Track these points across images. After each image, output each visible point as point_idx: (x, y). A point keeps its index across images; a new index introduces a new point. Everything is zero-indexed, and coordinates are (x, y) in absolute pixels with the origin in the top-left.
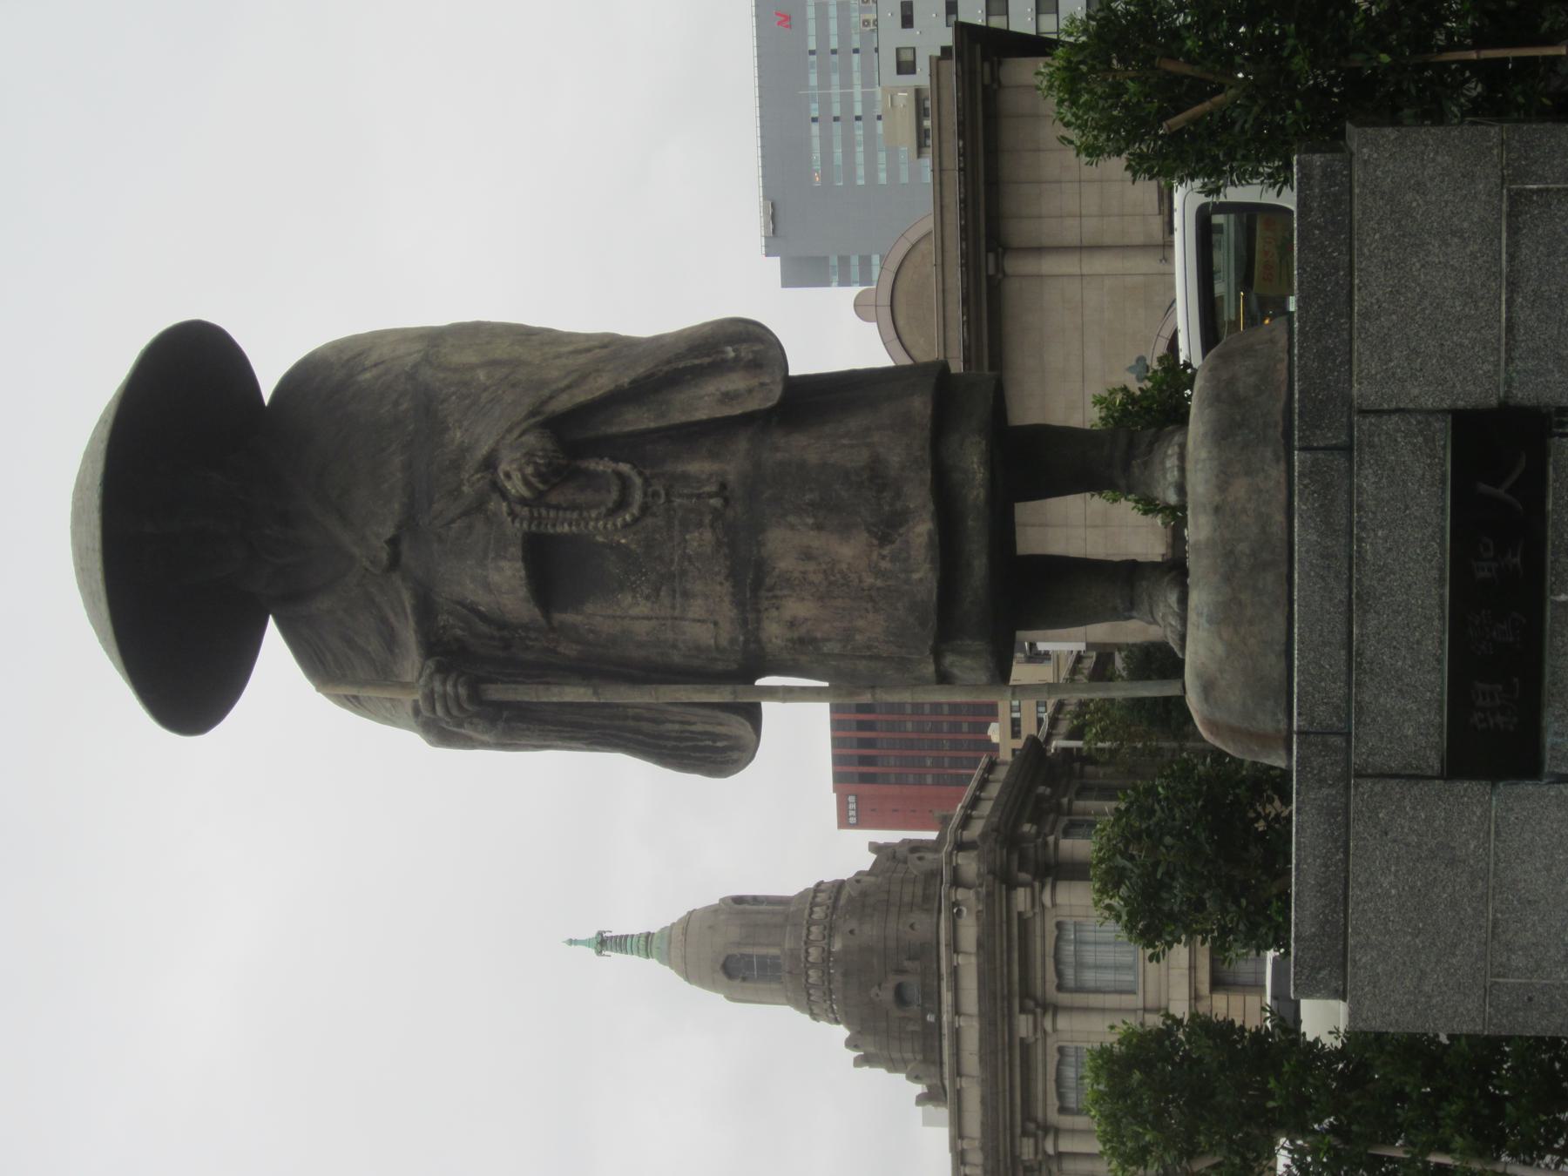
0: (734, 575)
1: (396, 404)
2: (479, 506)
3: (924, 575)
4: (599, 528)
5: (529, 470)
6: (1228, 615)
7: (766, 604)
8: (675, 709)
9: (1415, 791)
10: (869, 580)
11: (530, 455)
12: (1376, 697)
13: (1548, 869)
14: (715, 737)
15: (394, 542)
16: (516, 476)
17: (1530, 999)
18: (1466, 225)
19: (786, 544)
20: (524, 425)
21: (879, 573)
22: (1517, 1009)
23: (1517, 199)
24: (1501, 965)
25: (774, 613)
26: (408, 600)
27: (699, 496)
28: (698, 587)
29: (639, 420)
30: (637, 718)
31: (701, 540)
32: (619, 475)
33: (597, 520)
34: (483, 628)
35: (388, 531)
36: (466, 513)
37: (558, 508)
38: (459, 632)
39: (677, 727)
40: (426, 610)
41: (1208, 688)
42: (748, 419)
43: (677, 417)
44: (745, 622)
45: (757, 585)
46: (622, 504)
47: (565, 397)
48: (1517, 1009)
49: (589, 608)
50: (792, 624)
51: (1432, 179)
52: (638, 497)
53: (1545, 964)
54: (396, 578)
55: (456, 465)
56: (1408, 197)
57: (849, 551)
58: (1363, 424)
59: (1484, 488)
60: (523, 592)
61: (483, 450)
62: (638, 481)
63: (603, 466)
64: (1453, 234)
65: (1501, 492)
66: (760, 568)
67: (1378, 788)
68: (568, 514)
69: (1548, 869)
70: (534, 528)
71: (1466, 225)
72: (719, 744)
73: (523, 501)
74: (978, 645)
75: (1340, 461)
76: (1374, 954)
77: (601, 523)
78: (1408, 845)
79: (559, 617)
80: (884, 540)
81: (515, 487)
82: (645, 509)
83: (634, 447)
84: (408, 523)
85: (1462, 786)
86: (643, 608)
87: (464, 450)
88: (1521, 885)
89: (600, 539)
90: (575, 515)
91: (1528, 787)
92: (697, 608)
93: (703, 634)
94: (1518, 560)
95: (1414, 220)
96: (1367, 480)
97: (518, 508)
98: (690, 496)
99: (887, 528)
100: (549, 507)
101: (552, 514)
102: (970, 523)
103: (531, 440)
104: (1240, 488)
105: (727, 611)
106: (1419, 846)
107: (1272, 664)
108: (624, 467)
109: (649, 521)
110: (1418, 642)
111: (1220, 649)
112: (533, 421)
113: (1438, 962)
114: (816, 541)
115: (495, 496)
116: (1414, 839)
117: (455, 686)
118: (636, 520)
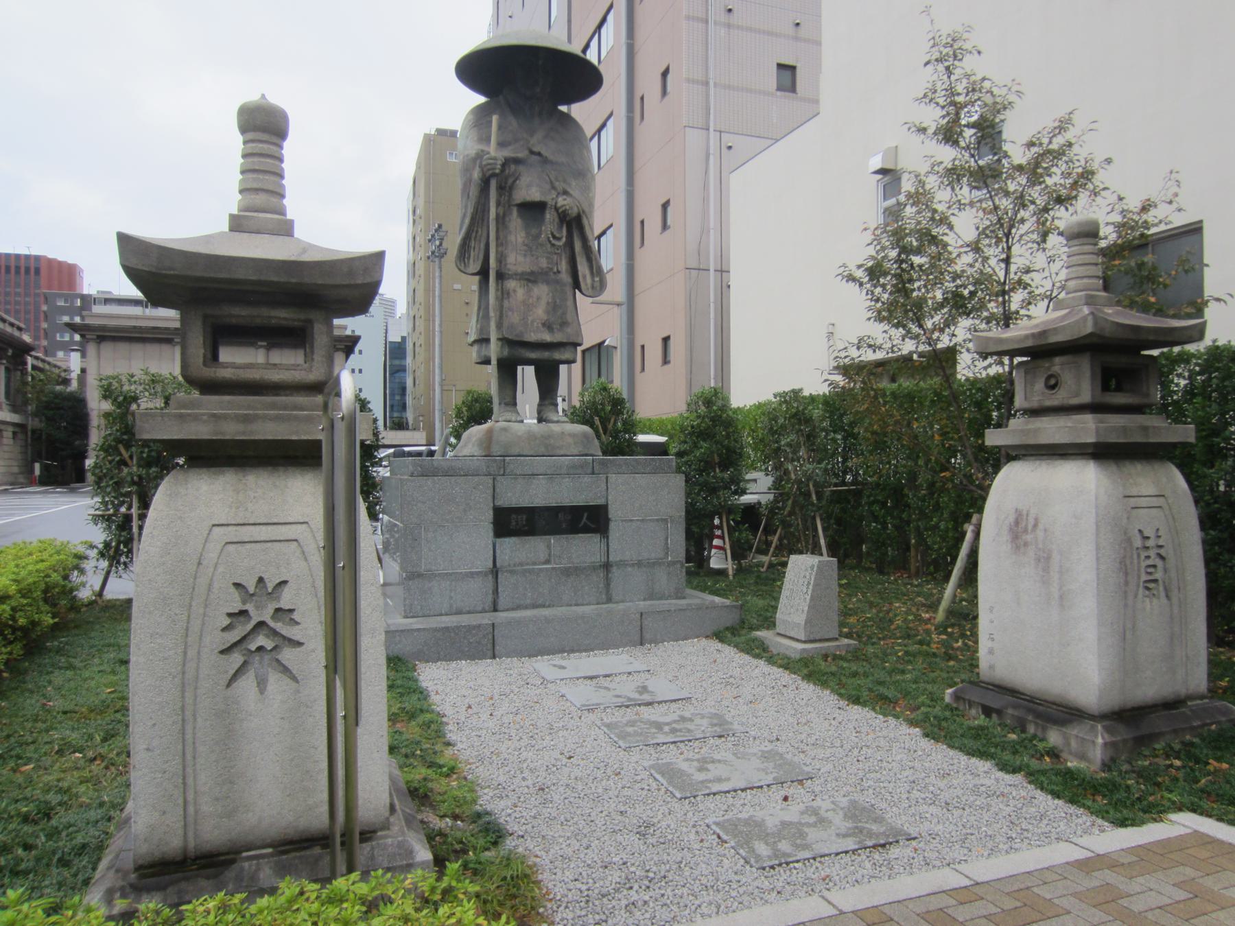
0: (532, 273)
2: (554, 188)
3: (532, 337)
6: (531, 436)
8: (482, 246)
10: (530, 318)
11: (571, 208)
19: (542, 291)
21: (533, 322)
23: (666, 520)
26: (520, 155)
28: (528, 259)
31: (544, 263)
40: (517, 161)
41: (505, 429)
44: (516, 274)
45: (529, 280)
46: (554, 237)
49: (519, 220)
50: (515, 291)
54: (526, 152)
55: (565, 181)
57: (540, 312)
58: (603, 477)
60: (528, 199)
66: (535, 282)
75: (590, 471)
79: (515, 211)
80: (544, 325)
82: (553, 245)
83: (570, 244)
85: (491, 513)
86: (520, 240)
87: (569, 185)
91: (491, 534)
92: (520, 259)
96: (587, 479)
99: (548, 326)
103: (575, 210)
104: (570, 440)
105: (520, 270)
107: (516, 451)
114: (543, 303)
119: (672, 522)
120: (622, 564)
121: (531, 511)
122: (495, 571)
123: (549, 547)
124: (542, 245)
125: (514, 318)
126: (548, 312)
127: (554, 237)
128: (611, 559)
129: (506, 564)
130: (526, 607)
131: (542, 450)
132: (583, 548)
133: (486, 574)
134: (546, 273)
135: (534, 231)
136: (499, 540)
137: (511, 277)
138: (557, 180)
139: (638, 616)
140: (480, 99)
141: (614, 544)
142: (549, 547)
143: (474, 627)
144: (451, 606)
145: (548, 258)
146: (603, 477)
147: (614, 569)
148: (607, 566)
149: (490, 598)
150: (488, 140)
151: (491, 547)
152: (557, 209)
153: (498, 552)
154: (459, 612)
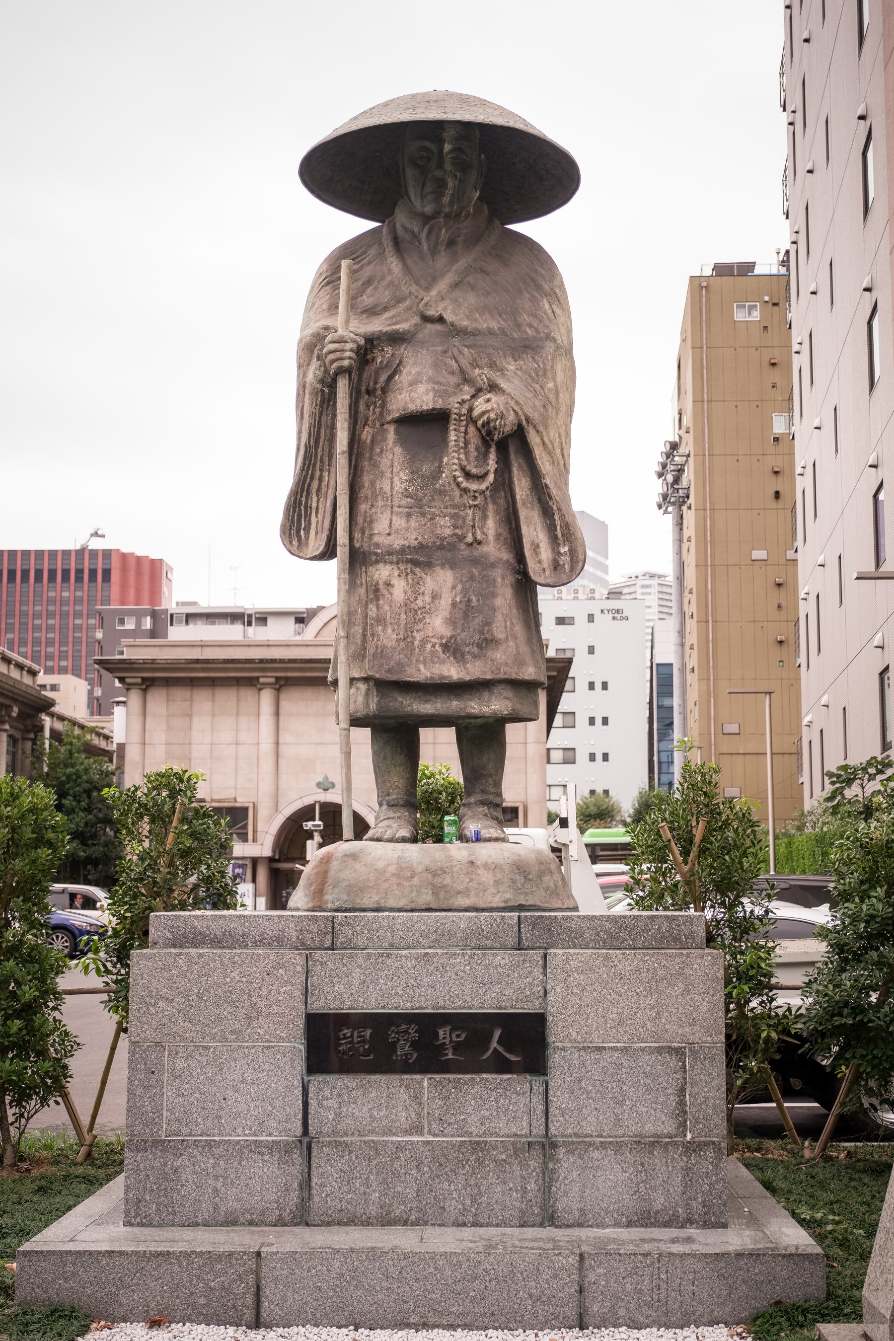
0: (421, 547)
1: (530, 326)
2: (466, 379)
3: (422, 673)
4: (453, 460)
5: (492, 416)
7: (403, 567)
8: (329, 503)
9: (298, 993)
10: (418, 636)
11: (502, 416)
12: (360, 967)
13: (243, 1081)
14: (307, 530)
15: (441, 320)
16: (488, 406)
17: (153, 1072)
18: (663, 1020)
19: (442, 582)
20: (520, 413)
21: (423, 642)
22: (146, 1064)
23: (677, 1051)
24: (177, 1052)
25: (396, 573)
26: (402, 327)
27: (474, 526)
28: (413, 524)
29: (522, 487)
30: (321, 479)
31: (445, 527)
32: (486, 474)
33: (459, 459)
34: (383, 378)
35: (449, 317)
36: (462, 371)
37: (466, 433)
38: (379, 360)
39: (314, 505)
40: (396, 339)
41: (353, 856)
42: (520, 558)
43: (523, 513)
44: (390, 554)
45: (415, 563)
46: (468, 475)
47: (538, 440)
48: (146, 1064)
49: (398, 450)
50: (388, 584)
51: (692, 999)
52: (473, 486)
53: (178, 1081)
54: (416, 319)
55: (492, 365)
56: (680, 984)
57: (438, 625)
58: (536, 955)
59: (497, 1033)
60: (412, 408)
61: (503, 385)
62: (483, 486)
63: (492, 463)
64: (658, 1013)
65: (494, 1044)
66: (427, 565)
67: (299, 968)
68: (462, 440)
69: (243, 1081)
70: (454, 416)
71: (663, 1020)
72: (302, 532)
73: (471, 410)
74: (373, 706)
75: (512, 941)
76: (185, 968)
77: (456, 461)
78: (260, 988)
79: (391, 429)
80: (446, 647)
81: (480, 406)
82: (465, 491)
83: (504, 483)
84: (457, 331)
86: (399, 487)
87: (502, 371)
88: (233, 1064)
89: (445, 460)
90: (462, 444)
91: (300, 1066)
92: (399, 522)
93: (381, 525)
94: (450, 1056)
95: (666, 988)
96: (503, 958)
97: (466, 406)
98: (473, 519)
99: (452, 649)
100: (467, 426)
101: (462, 429)
102: (454, 703)
103: (511, 417)
104: (486, 877)
105: (397, 542)
106: (259, 996)
107: (369, 900)
108: (491, 478)
109: (457, 493)
110: (396, 993)
111: (380, 865)
112: (523, 418)
113: (180, 1011)
114: (445, 602)
115: (473, 391)
116: (264, 992)
117: (350, 358)
118: (458, 485)
119: (695, 1054)
120: (581, 1145)
121: (427, 1024)
122: (306, 1142)
123: (417, 1097)
124: (442, 492)
125: (389, 637)
126: (451, 621)
127: (468, 475)
128: (553, 1130)
129: (328, 1128)
130: (367, 1223)
131: (426, 898)
132: (492, 1106)
133: (286, 1149)
134: (452, 547)
135: (426, 468)
136: (318, 1079)
137: (380, 559)
138: (474, 364)
139: (573, 1260)
141: (559, 1099)
142: (417, 1097)
143: (220, 1257)
144: (216, 1208)
145: (454, 516)
146: (536, 955)
147: (561, 1152)
148: (548, 1146)
149: (294, 1198)
150: (333, 307)
151: (298, 1092)
152: (472, 421)
153: (312, 1102)
154: (231, 1222)
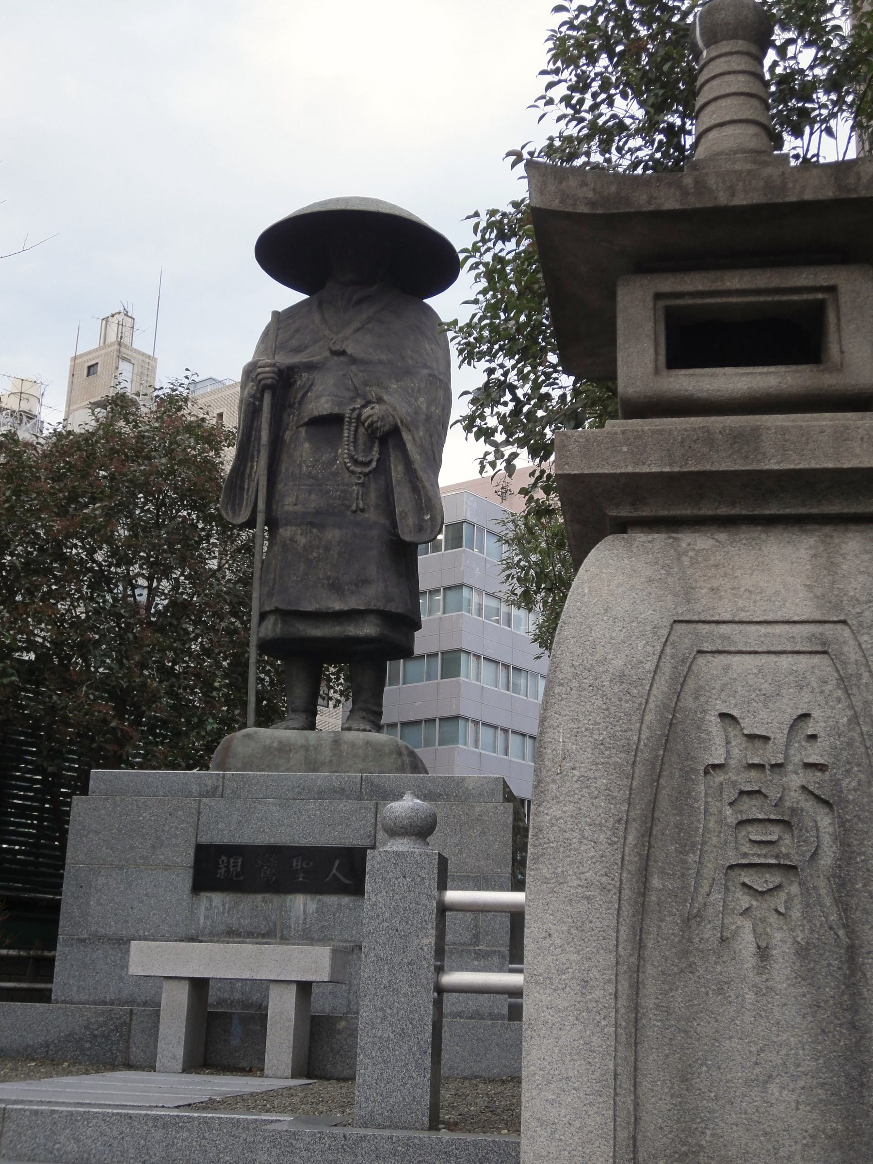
0: (317, 513)
1: (412, 358)
4: (343, 451)
5: (375, 419)
7: (304, 527)
9: (191, 829)
12: (238, 810)
13: (147, 895)
14: (240, 506)
15: (343, 353)
16: (371, 412)
17: (82, 887)
18: (464, 855)
20: (396, 416)
22: (77, 880)
24: (100, 872)
25: (299, 532)
27: (357, 499)
29: (397, 471)
30: (252, 467)
32: (371, 461)
33: (348, 450)
34: (299, 396)
35: (349, 351)
36: (356, 388)
37: (356, 431)
38: (299, 383)
39: (246, 487)
40: (311, 367)
42: (394, 525)
43: (397, 491)
45: (312, 524)
46: (356, 462)
47: (410, 437)
48: (77, 880)
51: (487, 840)
52: (359, 470)
53: (99, 894)
54: (327, 353)
55: (379, 385)
56: (478, 828)
58: (370, 805)
59: (337, 863)
60: (316, 413)
61: (385, 398)
62: (367, 470)
63: (375, 454)
64: (460, 850)
65: (334, 871)
67: (193, 811)
68: (352, 436)
69: (147, 895)
70: (347, 419)
71: (464, 855)
72: (237, 507)
73: (359, 415)
74: (278, 630)
76: (110, 809)
77: (346, 451)
78: (164, 825)
81: (367, 411)
83: (382, 469)
84: (354, 361)
85: (192, 852)
87: (386, 388)
88: (140, 881)
89: (340, 451)
90: (352, 440)
93: (289, 500)
94: (301, 879)
95: (468, 831)
97: (357, 412)
98: (357, 494)
100: (357, 428)
101: (352, 429)
102: (337, 628)
106: (163, 831)
108: (374, 464)
109: (347, 474)
110: (264, 831)
111: (268, 742)
112: (399, 421)
113: (104, 841)
115: (363, 402)
116: (167, 828)
117: (272, 378)
118: (348, 468)
127: (356, 462)
138: (365, 384)
140: (290, 297)
